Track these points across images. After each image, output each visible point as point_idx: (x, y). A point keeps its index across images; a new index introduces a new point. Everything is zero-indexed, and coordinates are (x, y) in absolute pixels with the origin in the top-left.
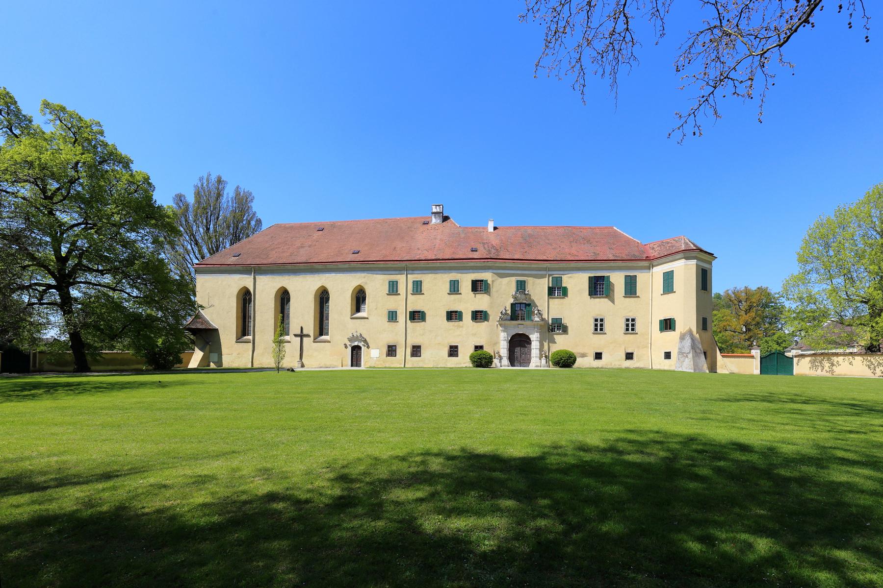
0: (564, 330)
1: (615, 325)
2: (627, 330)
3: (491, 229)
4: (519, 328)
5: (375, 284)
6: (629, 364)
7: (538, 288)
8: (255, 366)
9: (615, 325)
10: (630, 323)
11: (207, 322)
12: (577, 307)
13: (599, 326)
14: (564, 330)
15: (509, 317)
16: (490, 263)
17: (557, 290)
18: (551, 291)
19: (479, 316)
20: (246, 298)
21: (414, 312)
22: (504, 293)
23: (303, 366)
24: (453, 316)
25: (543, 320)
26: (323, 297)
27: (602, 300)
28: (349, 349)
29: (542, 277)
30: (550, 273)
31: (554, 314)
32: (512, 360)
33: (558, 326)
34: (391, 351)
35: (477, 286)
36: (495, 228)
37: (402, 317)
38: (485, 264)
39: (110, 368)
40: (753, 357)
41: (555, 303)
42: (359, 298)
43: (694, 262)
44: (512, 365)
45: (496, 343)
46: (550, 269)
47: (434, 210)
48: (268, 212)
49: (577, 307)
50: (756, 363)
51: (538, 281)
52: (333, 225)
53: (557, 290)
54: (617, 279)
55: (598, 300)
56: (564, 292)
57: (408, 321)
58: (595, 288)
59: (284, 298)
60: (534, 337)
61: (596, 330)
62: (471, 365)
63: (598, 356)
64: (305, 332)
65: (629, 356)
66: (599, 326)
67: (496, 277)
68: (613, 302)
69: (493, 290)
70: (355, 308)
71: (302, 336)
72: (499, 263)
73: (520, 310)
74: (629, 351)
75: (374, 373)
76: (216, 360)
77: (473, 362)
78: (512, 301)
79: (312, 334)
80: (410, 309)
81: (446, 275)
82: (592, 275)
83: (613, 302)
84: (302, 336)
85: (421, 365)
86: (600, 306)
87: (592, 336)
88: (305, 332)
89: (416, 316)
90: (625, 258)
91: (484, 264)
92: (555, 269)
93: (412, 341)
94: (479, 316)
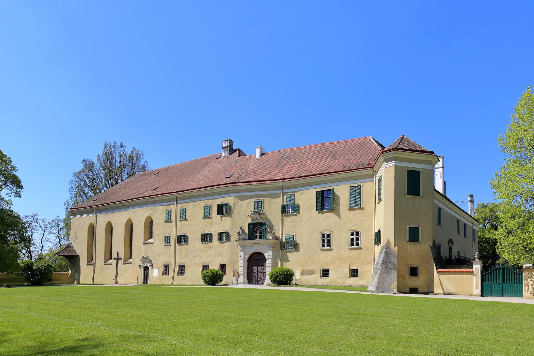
0: (296, 247)
1: (340, 240)
2: (352, 244)
3: (258, 156)
4: (254, 246)
5: (158, 213)
6: (353, 281)
7: (273, 209)
8: (95, 283)
9: (340, 240)
10: (326, 239)
11: (74, 251)
12: (307, 225)
13: (326, 241)
14: (296, 247)
15: (247, 237)
16: (232, 187)
17: (289, 209)
18: (284, 210)
19: (223, 237)
20: (92, 230)
21: (180, 236)
22: (243, 213)
23: (116, 283)
24: (206, 238)
25: (276, 238)
26: (130, 228)
27: (329, 214)
28: (142, 268)
29: (276, 196)
30: (285, 191)
31: (287, 232)
32: (250, 280)
33: (289, 245)
34: (166, 270)
35: (223, 210)
36: (262, 154)
37: (173, 241)
38: (228, 189)
39: (14, 283)
40: (472, 273)
41: (289, 220)
42: (150, 226)
43: (392, 164)
44: (250, 282)
45: (236, 262)
46: (283, 188)
47: (224, 145)
48: (154, 161)
49: (307, 225)
50: (477, 279)
51: (274, 200)
52: (166, 169)
53: (289, 209)
54: (342, 191)
55: (325, 214)
56: (296, 209)
57: (177, 245)
58: (323, 205)
59: (110, 228)
60: (268, 255)
61: (323, 246)
62: (202, 282)
63: (325, 273)
64: (119, 257)
65: (354, 273)
66: (326, 241)
67: (237, 200)
68: (339, 215)
69: (235, 212)
70: (148, 235)
71: (118, 259)
72: (238, 187)
73: (256, 230)
74: (354, 268)
75: (160, 289)
76: (77, 278)
77: (205, 281)
78: (249, 221)
79: (123, 258)
80: (178, 234)
81: (202, 202)
82: (321, 190)
83: (339, 215)
84: (118, 259)
85: (183, 282)
86: (327, 220)
87: (319, 252)
88: (119, 257)
89: (182, 239)
90: (352, 167)
91: (228, 189)
92: (285, 186)
93: (179, 262)
94: (223, 237)
